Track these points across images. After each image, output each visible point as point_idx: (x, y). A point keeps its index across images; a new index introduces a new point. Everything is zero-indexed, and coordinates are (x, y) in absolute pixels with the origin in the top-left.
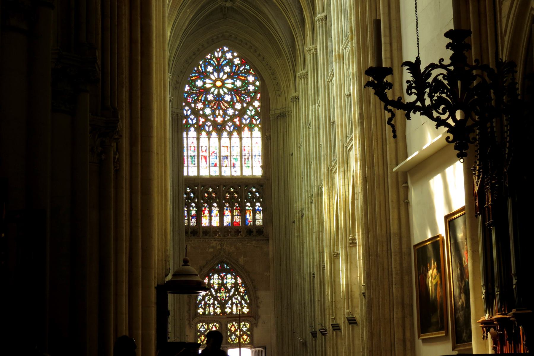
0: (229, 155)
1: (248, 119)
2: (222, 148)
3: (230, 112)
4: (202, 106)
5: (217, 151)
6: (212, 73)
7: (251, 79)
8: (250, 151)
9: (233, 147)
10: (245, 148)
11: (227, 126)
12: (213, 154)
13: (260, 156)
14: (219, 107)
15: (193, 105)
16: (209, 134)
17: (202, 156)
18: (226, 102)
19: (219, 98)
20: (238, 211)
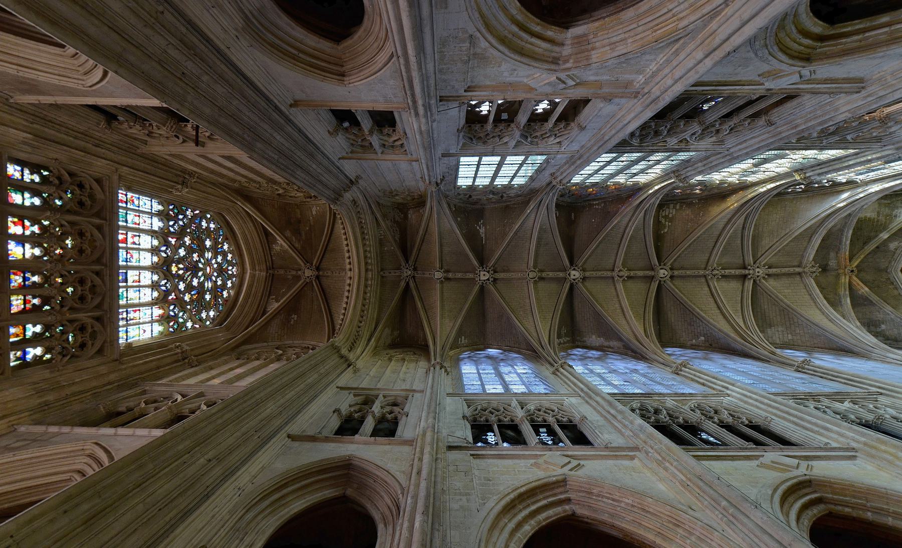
0: (130, 284)
1: (175, 313)
2: (137, 272)
3: (182, 286)
4: (187, 244)
5: (134, 263)
6: (217, 263)
7: (212, 313)
8: (134, 321)
9: (139, 291)
10: (138, 312)
11: (166, 281)
12: (129, 256)
13: (127, 339)
14: (186, 269)
15: (188, 230)
16: (154, 251)
17: (126, 234)
18: (192, 281)
19: (194, 269)
20: (22, 306)
